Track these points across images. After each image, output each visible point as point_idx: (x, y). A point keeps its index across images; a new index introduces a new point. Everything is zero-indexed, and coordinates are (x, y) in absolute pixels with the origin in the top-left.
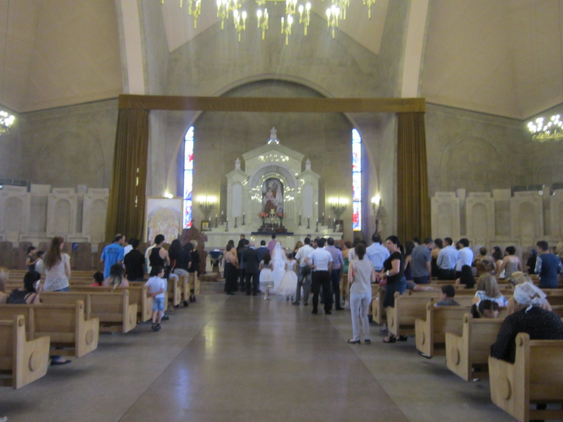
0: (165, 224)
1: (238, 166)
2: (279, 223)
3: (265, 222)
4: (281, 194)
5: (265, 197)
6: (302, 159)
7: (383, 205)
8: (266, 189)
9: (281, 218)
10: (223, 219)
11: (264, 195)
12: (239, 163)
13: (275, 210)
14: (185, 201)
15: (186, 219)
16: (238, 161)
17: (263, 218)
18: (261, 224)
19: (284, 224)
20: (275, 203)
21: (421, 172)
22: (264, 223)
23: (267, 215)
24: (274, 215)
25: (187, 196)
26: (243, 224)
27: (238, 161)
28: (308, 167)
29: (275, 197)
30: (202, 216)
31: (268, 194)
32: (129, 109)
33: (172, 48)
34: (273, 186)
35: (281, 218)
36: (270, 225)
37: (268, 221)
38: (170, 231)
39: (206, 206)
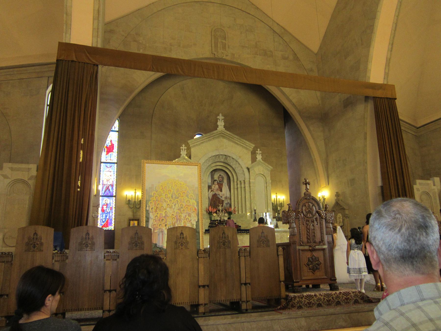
0: (175, 205)
1: (184, 153)
3: (213, 219)
4: (227, 187)
5: (210, 190)
6: (251, 149)
7: (341, 198)
8: (211, 181)
9: (230, 213)
11: (210, 187)
12: (185, 149)
13: (222, 206)
14: (101, 198)
15: (101, 218)
16: (183, 147)
17: (210, 213)
18: (209, 221)
20: (222, 197)
21: (402, 159)
22: (211, 220)
23: (215, 210)
24: (222, 211)
25: (103, 192)
28: (259, 157)
29: (221, 191)
30: (130, 214)
31: (213, 187)
32: (72, 61)
33: (107, 20)
34: (219, 178)
35: (230, 213)
37: (215, 217)
38: (183, 215)
39: (135, 202)
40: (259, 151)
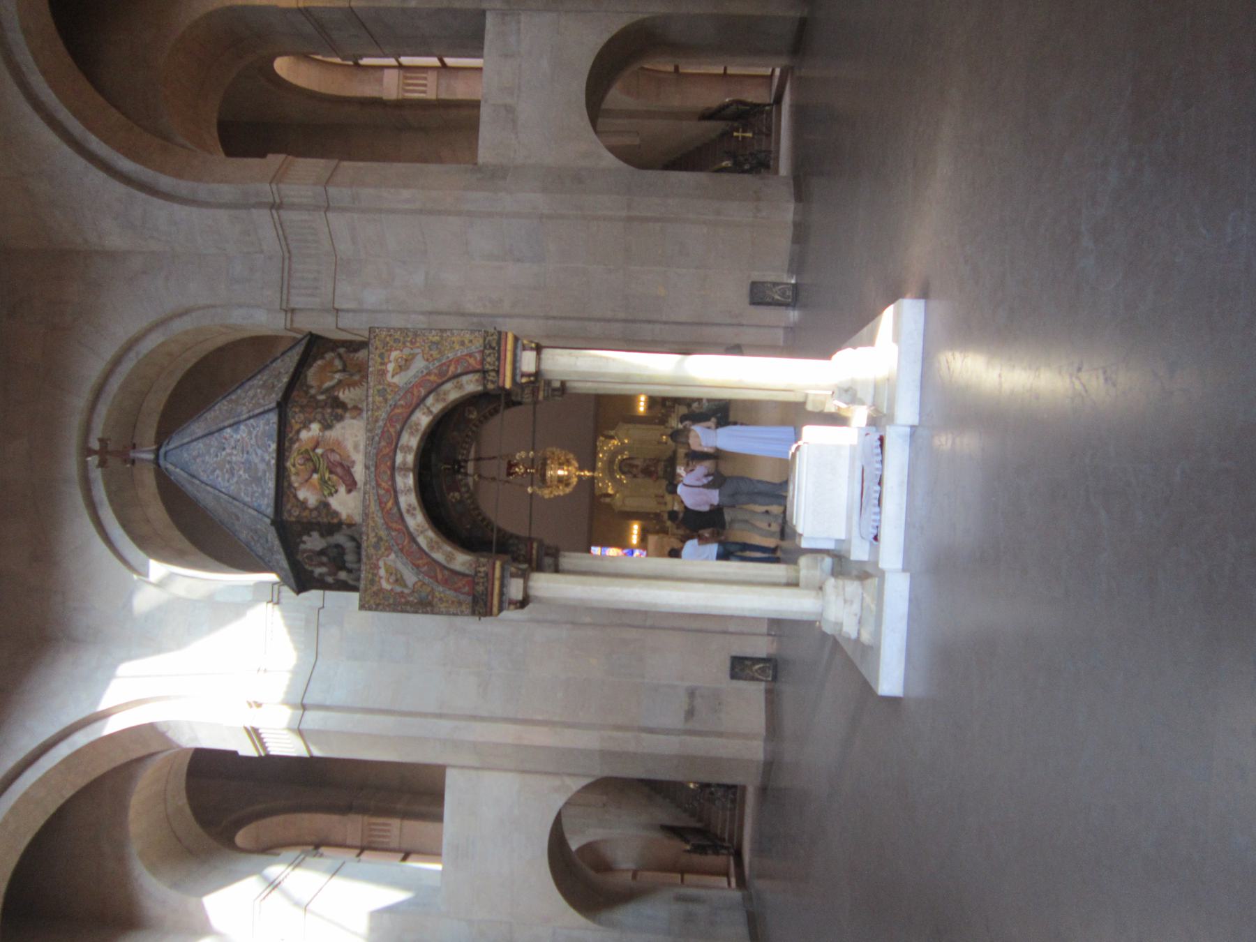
1: (608, 500)
2: (663, 463)
9: (659, 461)
10: (657, 516)
11: (635, 476)
16: (602, 500)
17: (657, 478)
19: (665, 458)
22: (664, 478)
26: (663, 497)
27: (602, 500)
28: (612, 433)
35: (659, 461)
36: (665, 471)
37: (661, 473)
40: (606, 433)
